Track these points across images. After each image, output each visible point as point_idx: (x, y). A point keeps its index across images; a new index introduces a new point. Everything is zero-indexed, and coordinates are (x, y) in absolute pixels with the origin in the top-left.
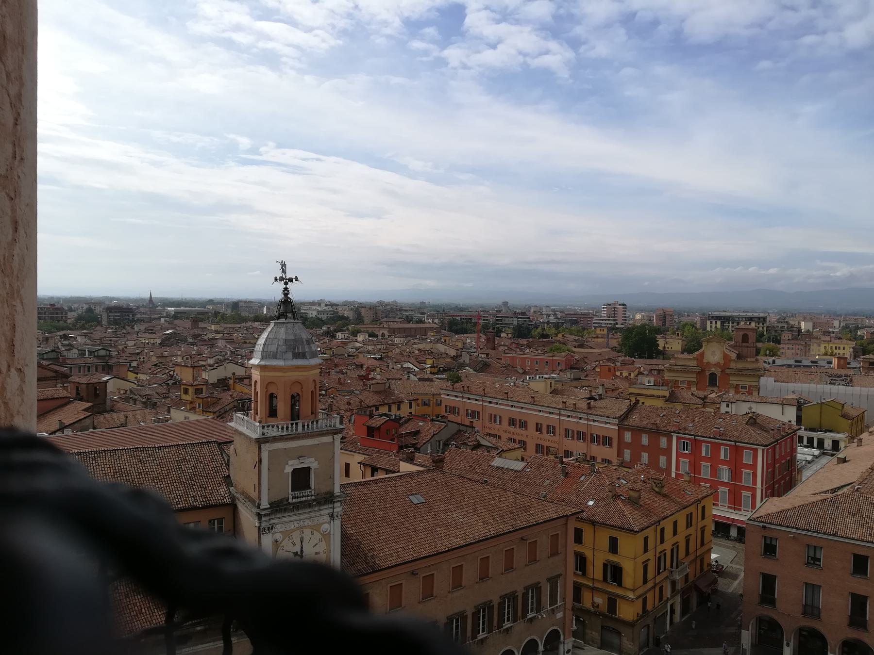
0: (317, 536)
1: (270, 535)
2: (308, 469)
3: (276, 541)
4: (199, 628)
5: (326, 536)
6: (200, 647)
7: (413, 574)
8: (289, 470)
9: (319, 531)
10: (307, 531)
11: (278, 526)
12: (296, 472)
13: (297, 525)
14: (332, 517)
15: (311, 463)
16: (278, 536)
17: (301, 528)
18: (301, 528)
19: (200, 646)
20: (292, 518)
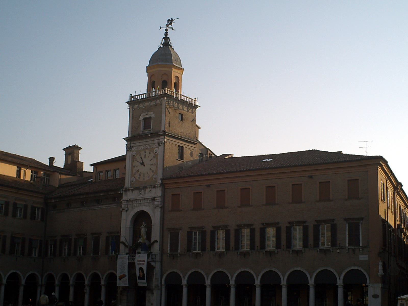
0: (152, 155)
1: (131, 152)
2: (150, 118)
3: (134, 156)
4: (101, 195)
5: (156, 155)
6: (104, 206)
7: (208, 186)
8: (141, 118)
9: (153, 153)
10: (147, 152)
11: (134, 148)
12: (144, 119)
13: (143, 148)
14: (159, 144)
15: (151, 114)
16: (134, 153)
17: (145, 149)
18: (145, 149)
19: (104, 206)
20: (141, 144)
